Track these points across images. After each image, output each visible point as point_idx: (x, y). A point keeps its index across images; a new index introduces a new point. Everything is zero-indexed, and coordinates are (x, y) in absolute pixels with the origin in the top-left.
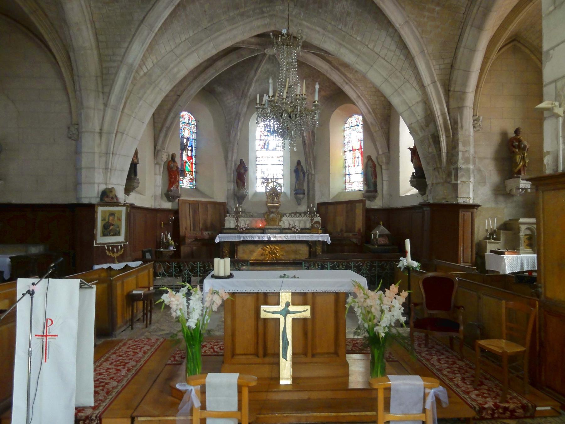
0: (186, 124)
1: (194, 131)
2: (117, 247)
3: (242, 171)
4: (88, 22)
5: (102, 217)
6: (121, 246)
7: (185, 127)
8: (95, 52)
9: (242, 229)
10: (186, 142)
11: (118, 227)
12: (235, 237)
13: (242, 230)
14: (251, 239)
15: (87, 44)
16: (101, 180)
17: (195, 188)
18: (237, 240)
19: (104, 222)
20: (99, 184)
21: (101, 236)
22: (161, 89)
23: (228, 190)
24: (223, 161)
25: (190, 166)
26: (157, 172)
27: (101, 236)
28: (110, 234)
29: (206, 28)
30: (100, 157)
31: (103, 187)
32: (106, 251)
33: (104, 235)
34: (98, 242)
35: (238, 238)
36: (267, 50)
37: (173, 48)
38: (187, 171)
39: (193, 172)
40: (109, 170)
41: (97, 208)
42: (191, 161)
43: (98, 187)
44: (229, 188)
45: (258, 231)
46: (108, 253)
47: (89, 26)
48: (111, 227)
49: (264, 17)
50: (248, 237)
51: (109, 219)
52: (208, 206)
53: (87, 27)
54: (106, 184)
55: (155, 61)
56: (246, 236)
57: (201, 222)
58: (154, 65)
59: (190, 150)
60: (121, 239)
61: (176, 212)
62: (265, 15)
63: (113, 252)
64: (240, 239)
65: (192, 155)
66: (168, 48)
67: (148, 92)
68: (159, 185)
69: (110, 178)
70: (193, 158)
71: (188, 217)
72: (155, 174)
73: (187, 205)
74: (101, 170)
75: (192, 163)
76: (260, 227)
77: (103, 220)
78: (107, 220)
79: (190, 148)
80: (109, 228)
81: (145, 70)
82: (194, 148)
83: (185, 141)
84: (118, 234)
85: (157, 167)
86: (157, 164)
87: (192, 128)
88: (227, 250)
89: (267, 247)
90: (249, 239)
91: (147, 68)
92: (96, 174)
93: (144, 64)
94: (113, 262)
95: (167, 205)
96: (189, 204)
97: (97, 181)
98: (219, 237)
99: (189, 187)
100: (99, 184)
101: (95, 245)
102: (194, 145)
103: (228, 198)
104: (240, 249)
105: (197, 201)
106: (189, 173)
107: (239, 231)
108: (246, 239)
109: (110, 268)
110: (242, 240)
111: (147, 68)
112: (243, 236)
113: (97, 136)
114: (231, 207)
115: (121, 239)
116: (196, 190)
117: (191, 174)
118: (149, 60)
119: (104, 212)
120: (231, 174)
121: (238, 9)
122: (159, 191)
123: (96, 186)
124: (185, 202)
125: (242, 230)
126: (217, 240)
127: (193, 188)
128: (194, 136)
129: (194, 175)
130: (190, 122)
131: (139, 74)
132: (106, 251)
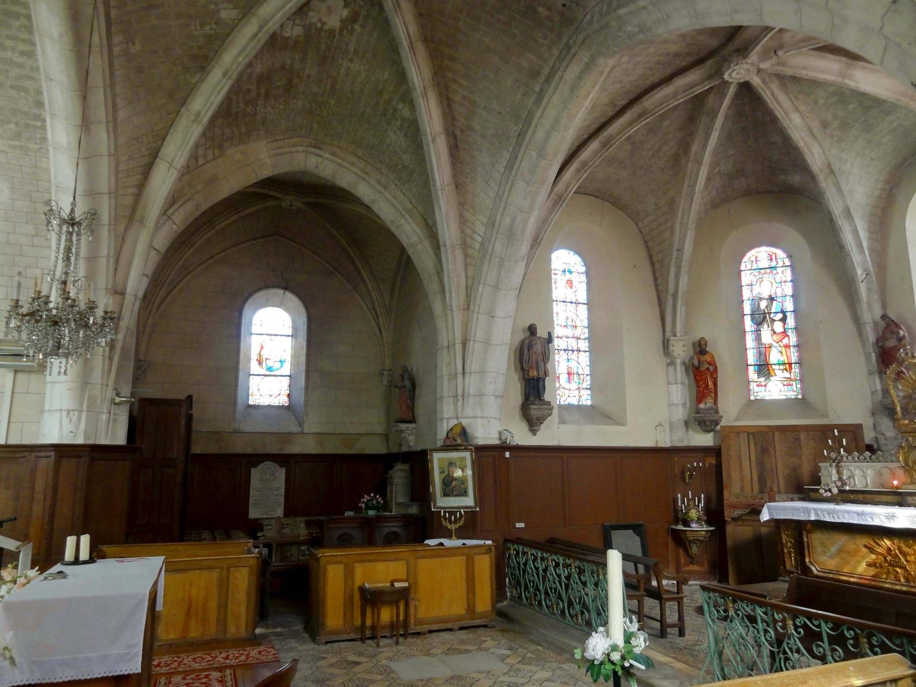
0: (762, 271)
1: (784, 279)
2: (454, 513)
3: (891, 343)
4: (404, 213)
5: (440, 467)
6: (460, 512)
7: (761, 276)
8: (427, 244)
9: (830, 490)
10: (766, 307)
11: (463, 484)
12: (797, 509)
13: (829, 494)
14: (834, 518)
15: (414, 239)
16: (451, 414)
17: (800, 397)
18: (802, 517)
19: (443, 476)
20: (448, 419)
21: (441, 497)
22: (501, 258)
23: (873, 393)
24: (853, 330)
25: (781, 353)
26: (672, 379)
27: (441, 497)
28: (453, 493)
29: (519, 135)
30: (450, 380)
31: (453, 422)
32: (442, 519)
33: (445, 495)
34: (439, 504)
35: (804, 513)
36: (730, 75)
37: (496, 190)
38: (775, 364)
39: (790, 364)
40: (460, 398)
41: (432, 455)
42: (785, 341)
43: (448, 423)
44: (874, 390)
45: (890, 498)
46: (444, 522)
47: (407, 216)
48: (454, 483)
49: (575, 55)
50: (825, 512)
51: (449, 471)
52: (803, 436)
53: (406, 220)
54: (457, 418)
55: (485, 221)
56: (822, 510)
57: (782, 472)
58: (486, 227)
59: (780, 320)
60: (469, 501)
61: (716, 452)
62: (573, 51)
63: (451, 522)
64: (809, 516)
65: (785, 329)
66: (492, 194)
67: (485, 269)
68: (676, 402)
69: (463, 409)
70: (790, 333)
71: (746, 464)
72: (669, 383)
73: (743, 438)
74: (451, 400)
75: (787, 346)
76: (893, 487)
77: (442, 472)
78: (446, 473)
79: (780, 316)
80: (451, 484)
81: (479, 239)
82: (788, 314)
83: (763, 304)
84: (464, 493)
85: (671, 368)
86: (672, 363)
87: (780, 274)
88: (791, 542)
89: (879, 545)
90: (828, 519)
91: (479, 235)
92: (445, 406)
93: (474, 232)
94: (449, 536)
95: (705, 440)
96: (748, 434)
97: (445, 415)
98: (769, 508)
99: (785, 397)
100: (448, 419)
101: (433, 510)
102: (789, 306)
103: (873, 414)
104: (816, 539)
105: (769, 427)
106: (782, 367)
107: (822, 494)
108: (822, 519)
109: (441, 544)
110: (813, 518)
111: (479, 235)
112: (815, 510)
113: (445, 352)
114: (883, 435)
115: (469, 501)
116: (801, 404)
117: (786, 369)
118: (478, 223)
119: (439, 459)
120: (870, 354)
121: (538, 73)
122: (680, 414)
123: (445, 421)
124: (737, 431)
125: (829, 494)
126: (765, 516)
127: (796, 399)
128: (788, 289)
129: (796, 369)
130: (774, 264)
131: (474, 249)
132: (442, 519)
